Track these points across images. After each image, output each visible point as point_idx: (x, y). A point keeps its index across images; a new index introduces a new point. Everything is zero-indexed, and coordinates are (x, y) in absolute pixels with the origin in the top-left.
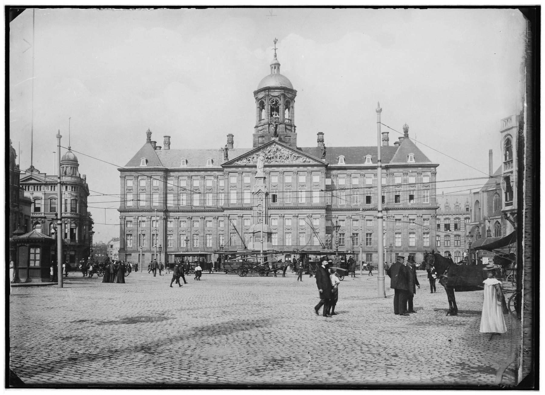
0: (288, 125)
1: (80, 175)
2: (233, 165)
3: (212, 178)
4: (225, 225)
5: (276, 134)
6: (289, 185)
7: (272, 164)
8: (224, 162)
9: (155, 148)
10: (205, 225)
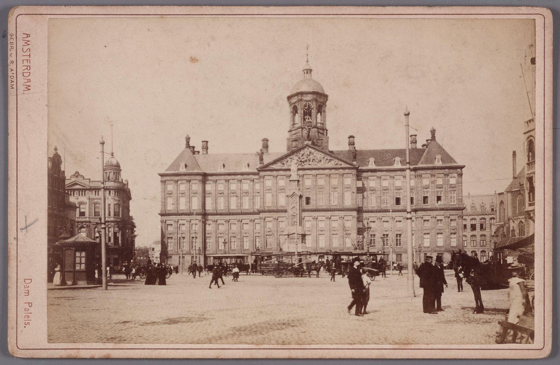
0: (320, 129)
1: (122, 180)
2: (268, 168)
3: (249, 181)
4: (261, 227)
5: (309, 138)
6: (321, 188)
7: (306, 166)
8: (259, 166)
9: (194, 153)
10: (242, 228)
